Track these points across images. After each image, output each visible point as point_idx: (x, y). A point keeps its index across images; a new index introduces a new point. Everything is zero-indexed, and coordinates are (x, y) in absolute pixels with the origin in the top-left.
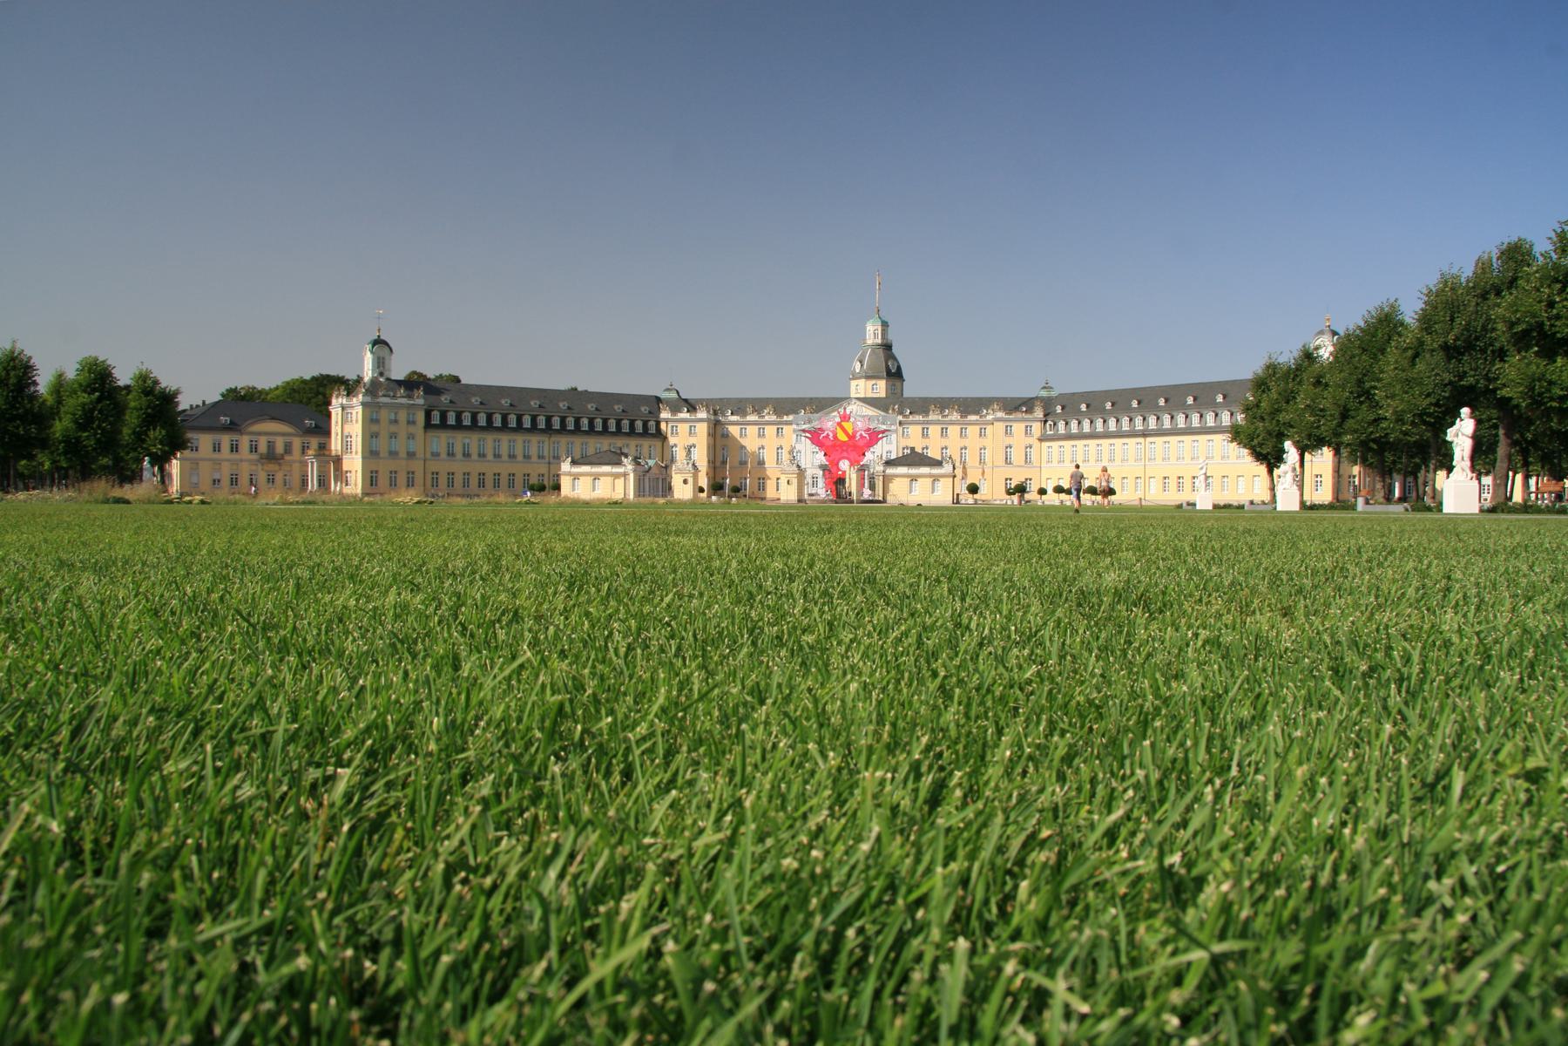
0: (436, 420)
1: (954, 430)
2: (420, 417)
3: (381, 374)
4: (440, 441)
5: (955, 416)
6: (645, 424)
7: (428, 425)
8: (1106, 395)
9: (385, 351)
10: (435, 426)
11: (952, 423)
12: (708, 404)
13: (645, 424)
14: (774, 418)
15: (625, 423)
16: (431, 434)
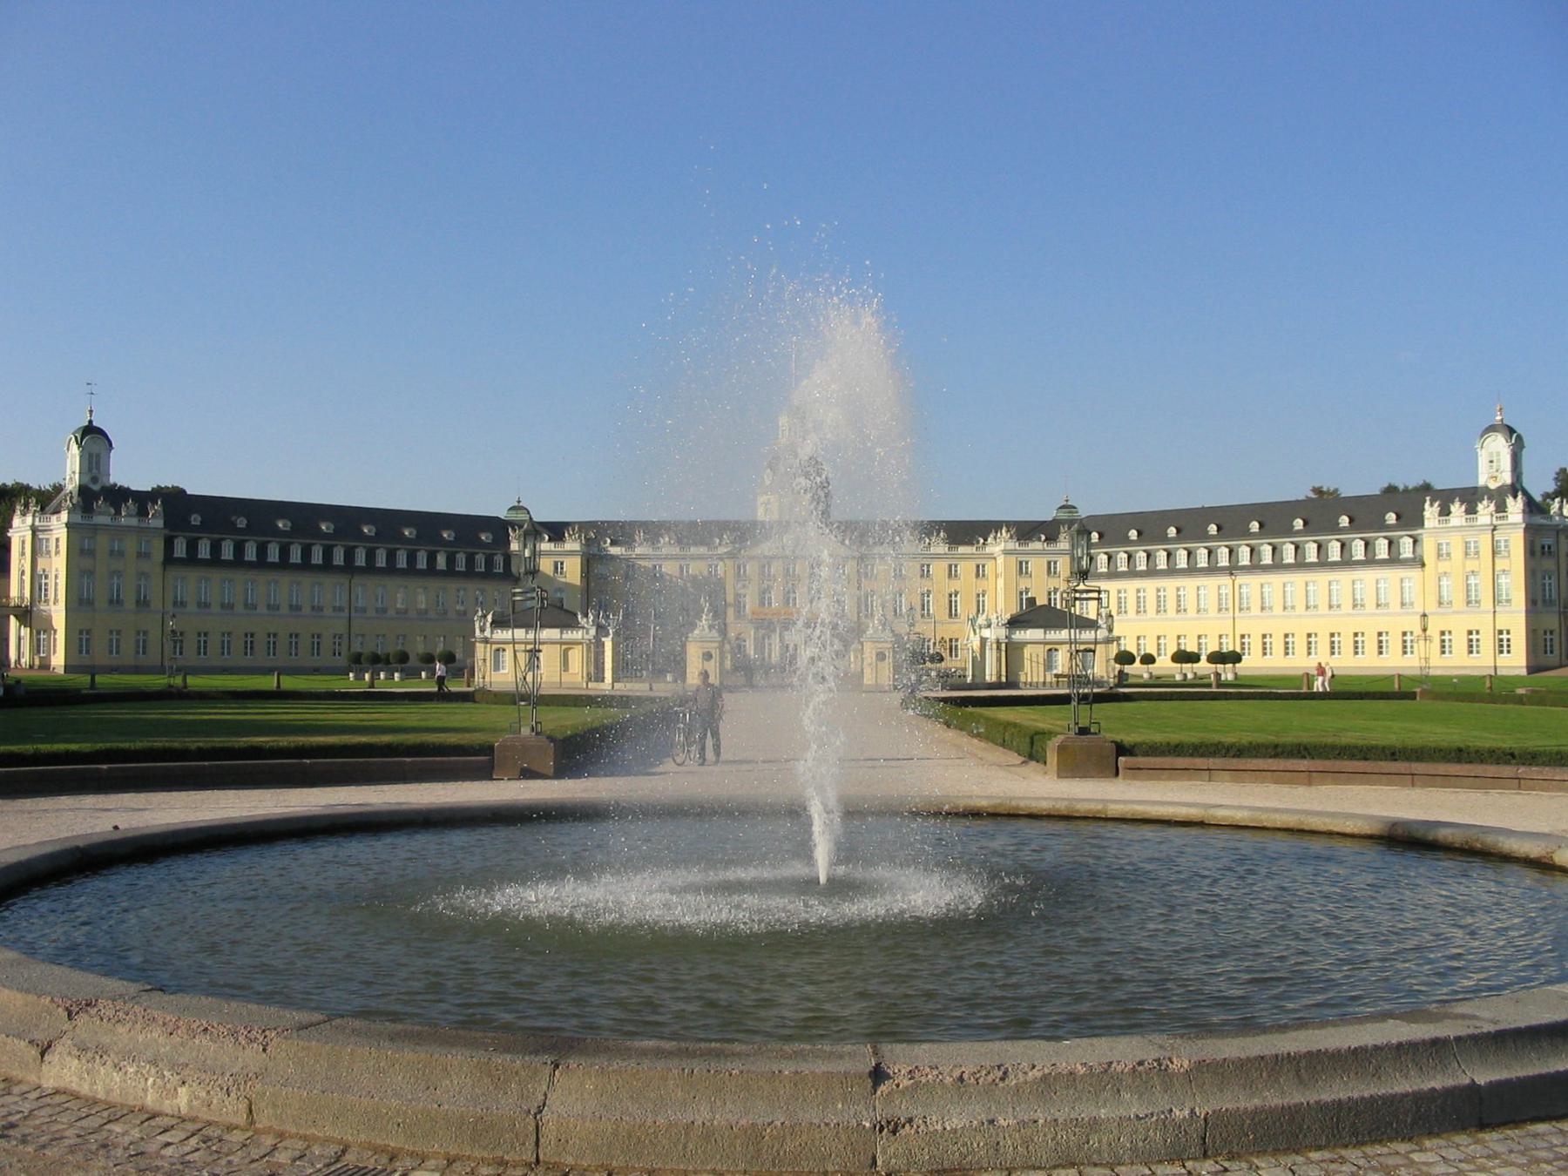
0: (180, 550)
1: (938, 569)
2: (158, 546)
3: (95, 480)
4: (190, 583)
5: (941, 548)
6: (489, 562)
7: (169, 560)
8: (1166, 517)
9: (97, 446)
10: (181, 562)
11: (938, 557)
12: (584, 526)
13: (489, 562)
14: (675, 550)
15: (461, 558)
16: (174, 572)
